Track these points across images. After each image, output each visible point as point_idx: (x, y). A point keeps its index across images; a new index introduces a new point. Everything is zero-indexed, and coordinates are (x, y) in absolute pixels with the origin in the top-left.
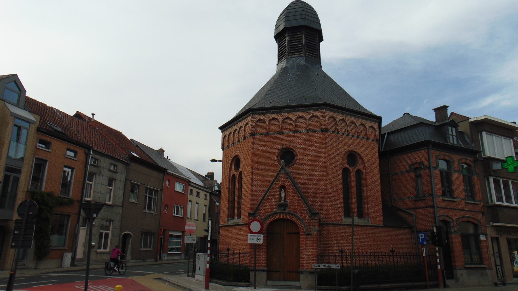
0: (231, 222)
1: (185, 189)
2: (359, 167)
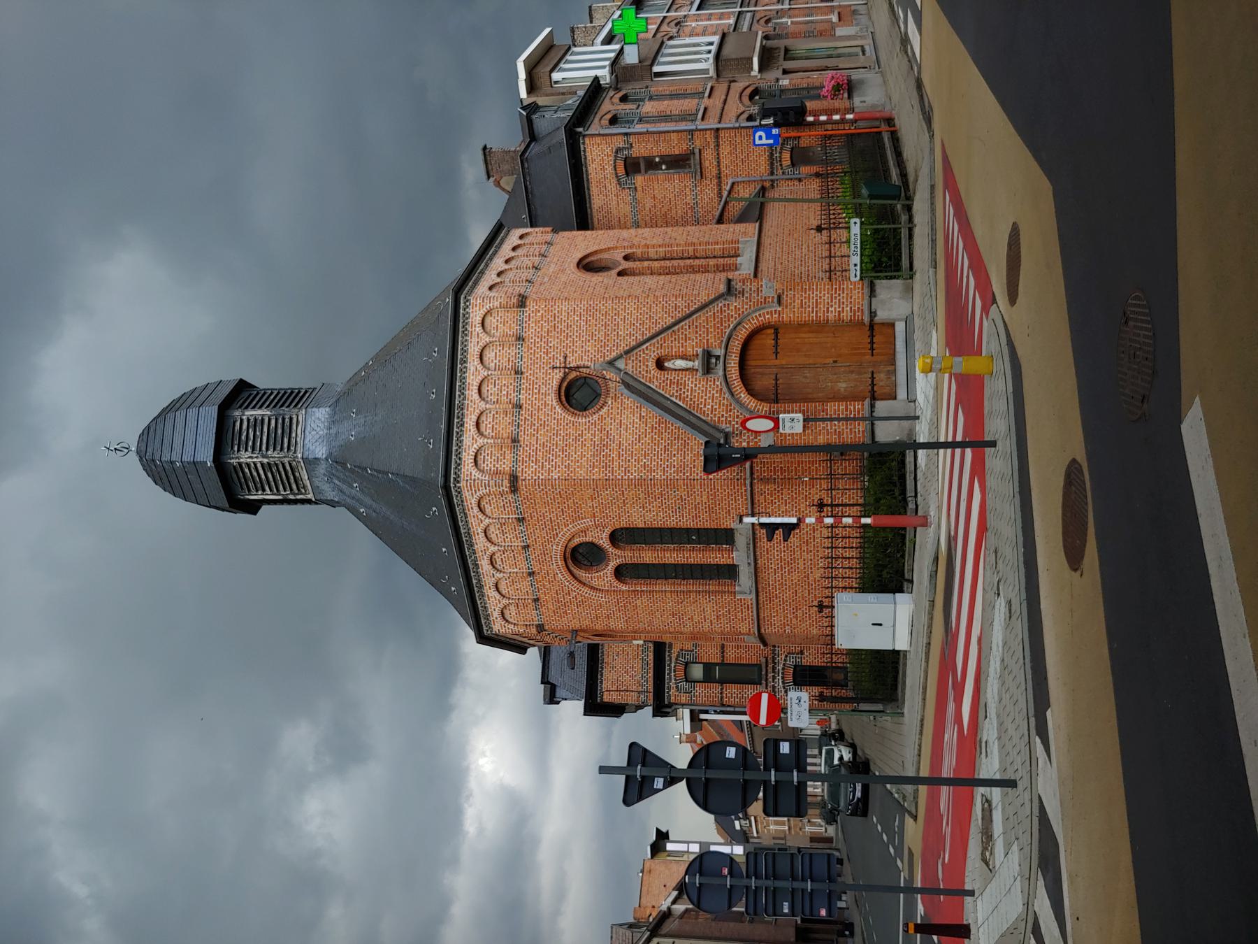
0: (746, 577)
2: (618, 256)
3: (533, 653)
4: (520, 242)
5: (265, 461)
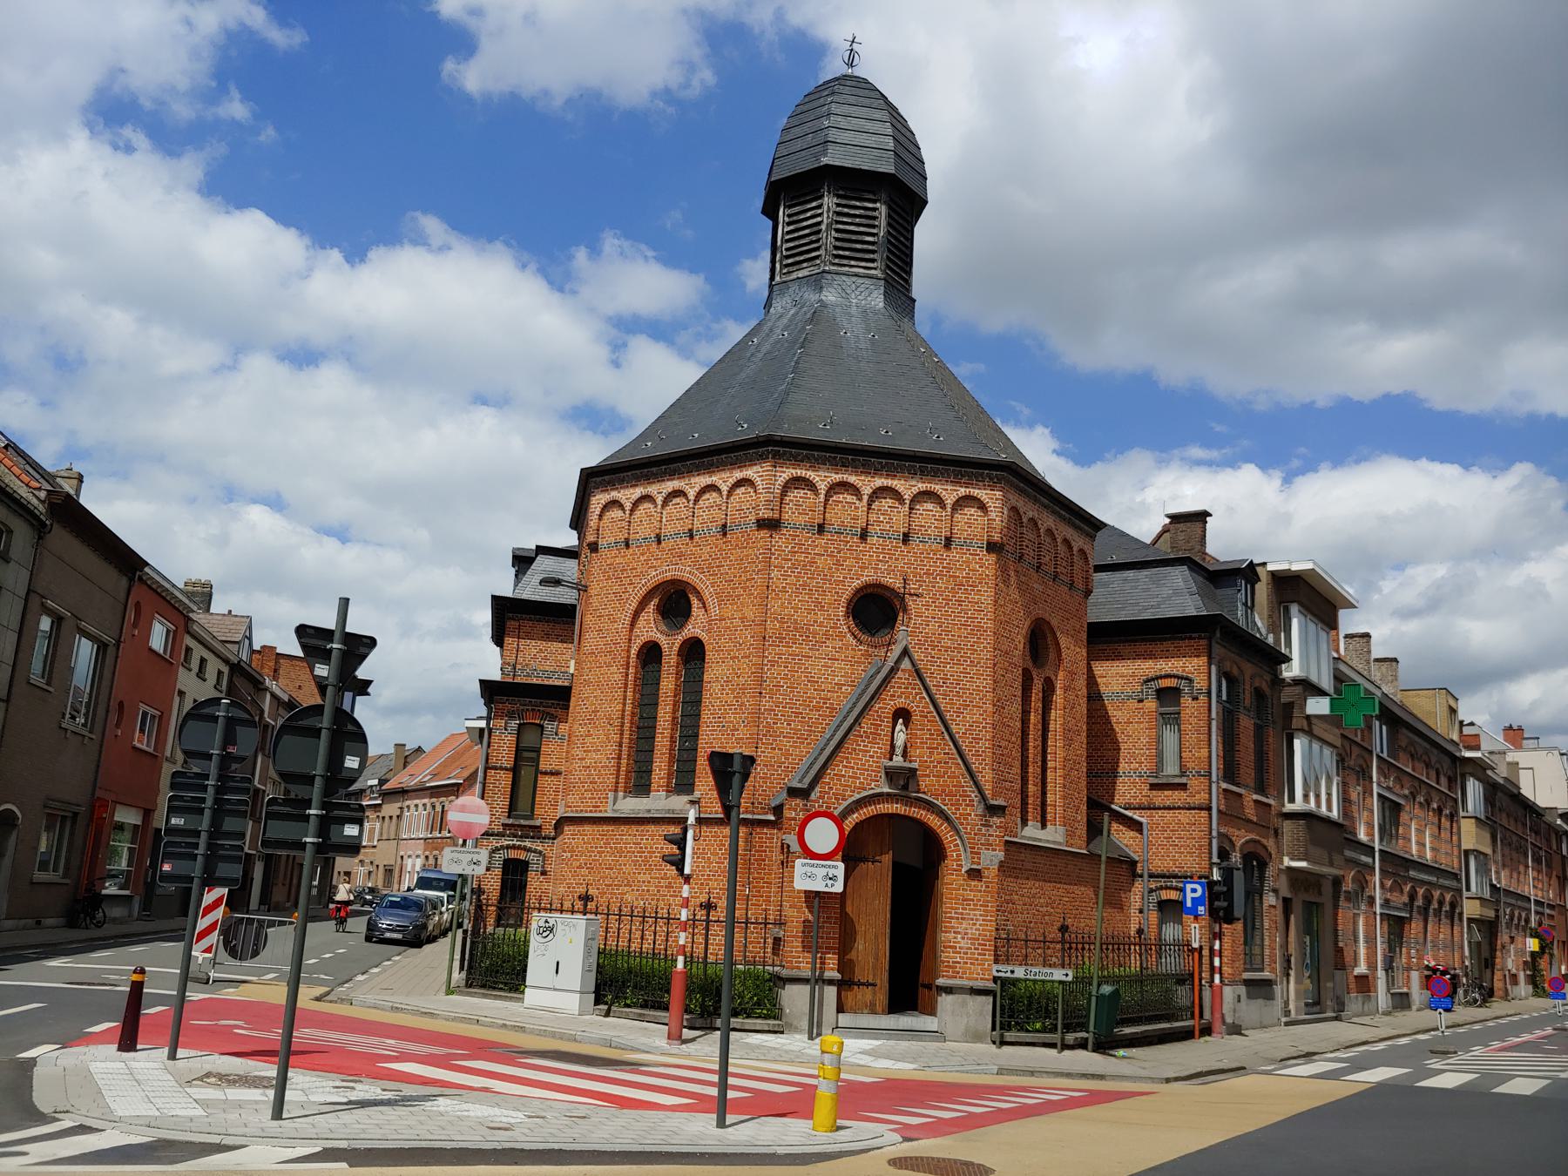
0: (631, 805)
1: (173, 638)
3: (569, 539)
4: (1075, 549)
5: (823, 227)
